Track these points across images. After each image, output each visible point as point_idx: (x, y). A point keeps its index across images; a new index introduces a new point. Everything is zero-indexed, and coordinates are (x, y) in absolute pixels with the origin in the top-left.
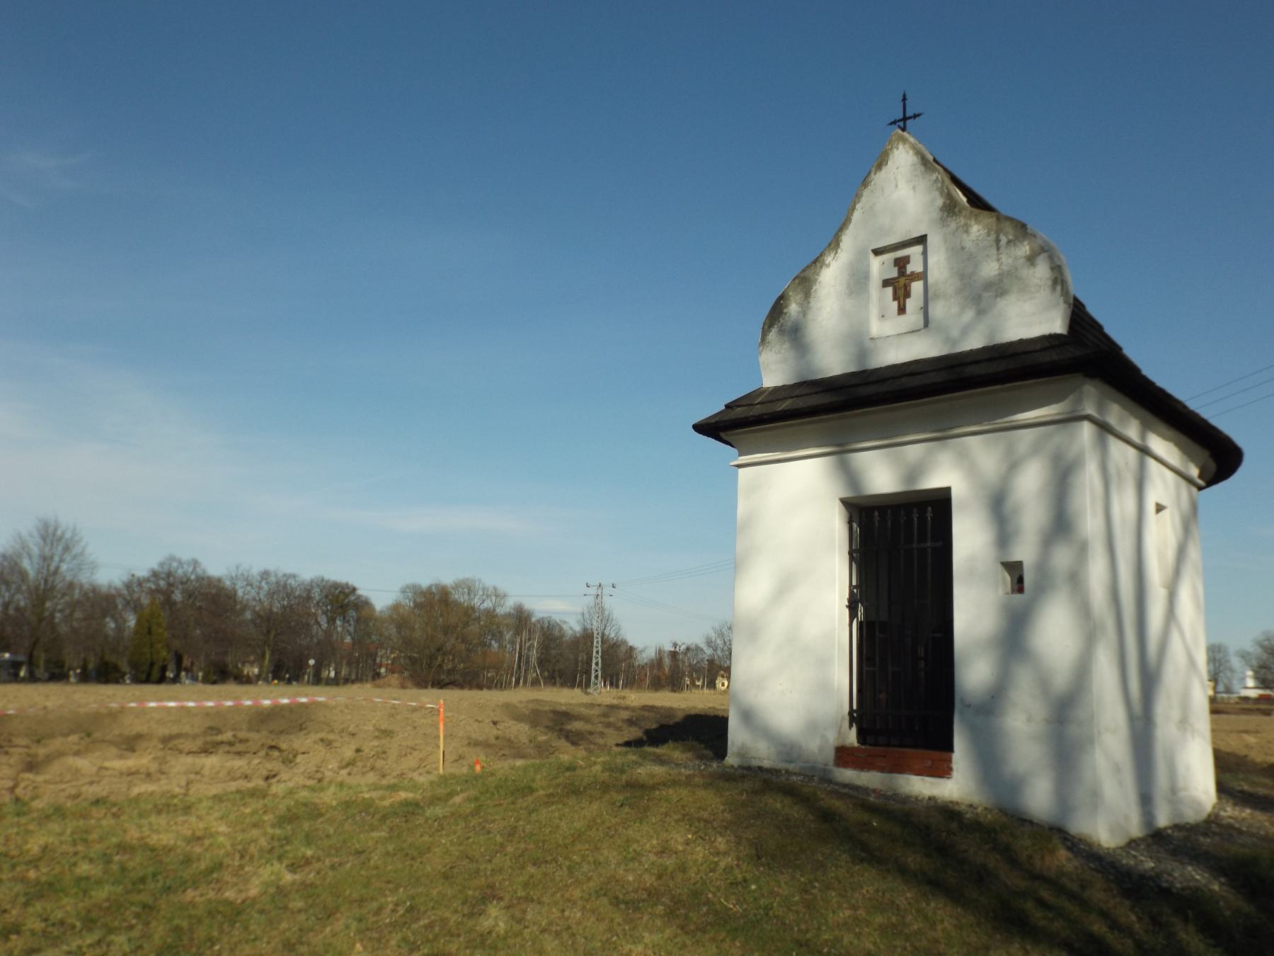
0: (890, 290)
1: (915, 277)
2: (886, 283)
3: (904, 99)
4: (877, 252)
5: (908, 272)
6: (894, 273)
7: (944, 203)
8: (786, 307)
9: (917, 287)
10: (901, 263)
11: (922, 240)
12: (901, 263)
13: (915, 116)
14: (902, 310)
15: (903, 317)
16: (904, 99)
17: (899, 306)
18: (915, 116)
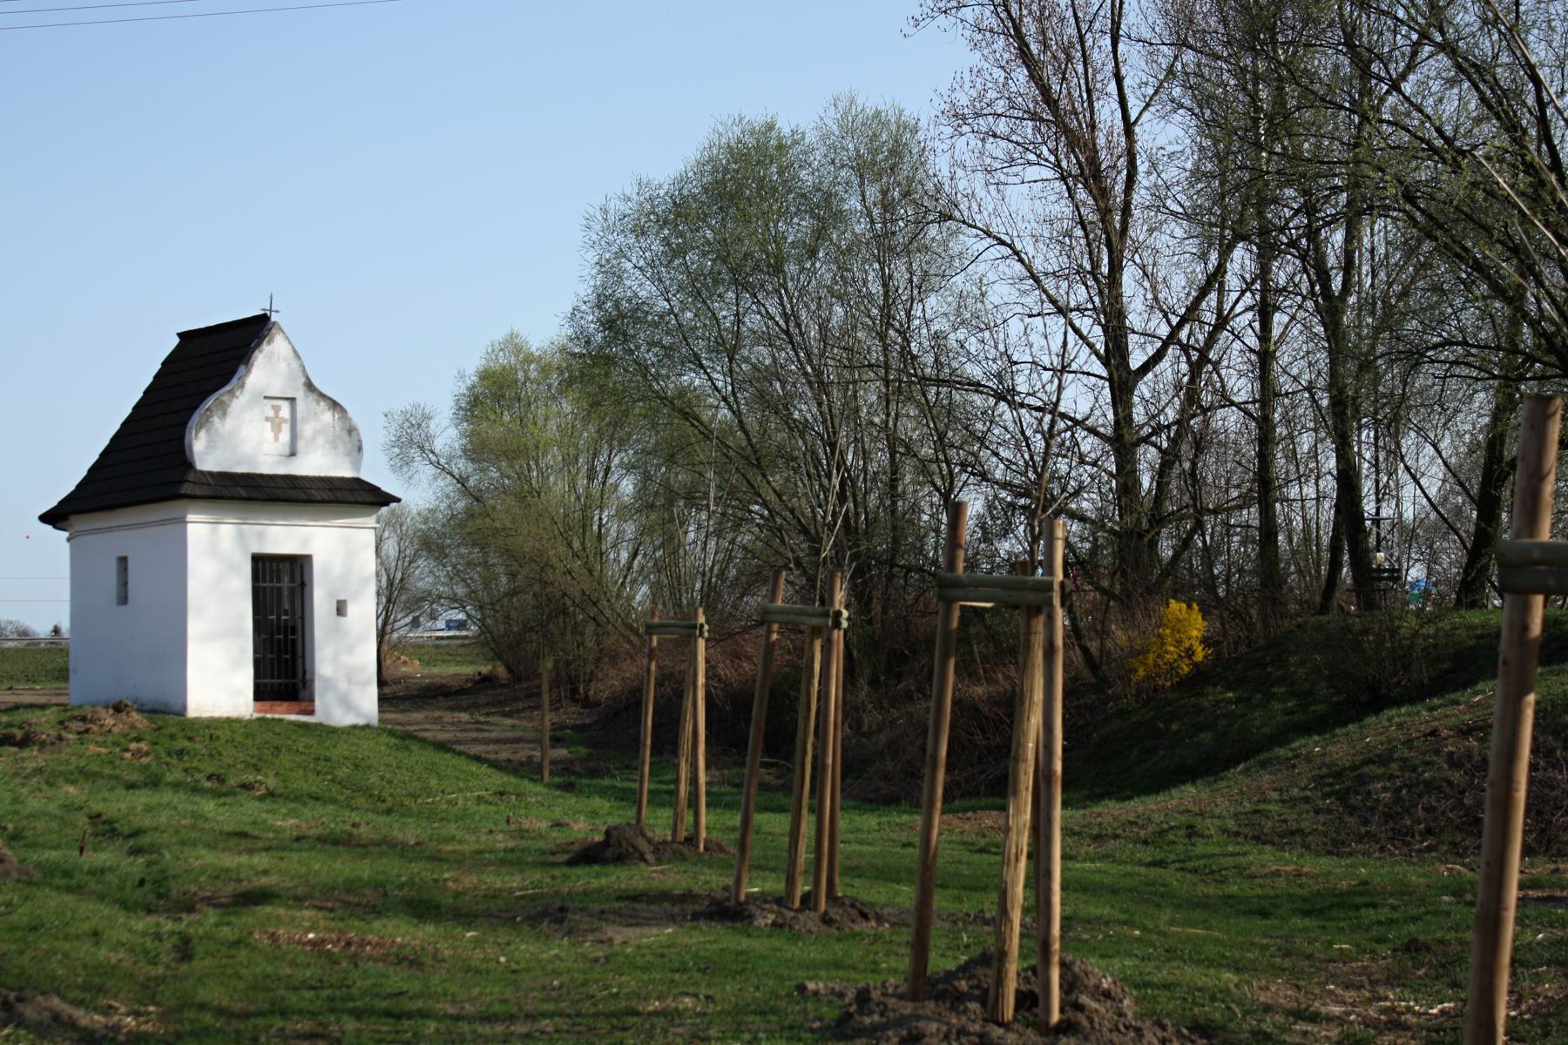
6: (271, 413)
10: (277, 409)
11: (292, 400)
14: (276, 439)
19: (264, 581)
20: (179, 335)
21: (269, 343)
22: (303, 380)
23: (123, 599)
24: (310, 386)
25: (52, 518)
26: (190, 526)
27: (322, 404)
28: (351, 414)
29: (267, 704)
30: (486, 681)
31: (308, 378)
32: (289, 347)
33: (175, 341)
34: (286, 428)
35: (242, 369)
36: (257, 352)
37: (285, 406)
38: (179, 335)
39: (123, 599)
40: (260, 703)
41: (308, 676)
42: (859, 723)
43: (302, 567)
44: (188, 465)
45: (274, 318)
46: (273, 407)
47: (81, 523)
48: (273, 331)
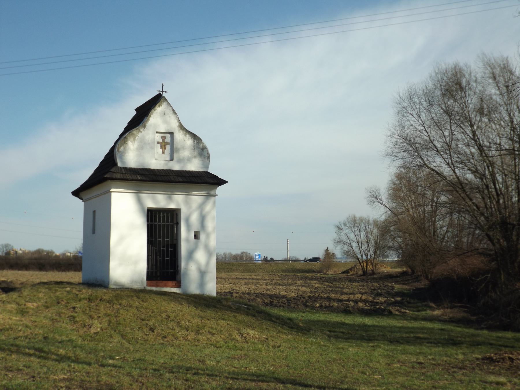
0: (159, 145)
1: (167, 143)
2: (158, 143)
3: (163, 85)
4: (157, 132)
5: (166, 141)
6: (161, 140)
7: (179, 126)
8: (127, 141)
9: (168, 147)
11: (172, 134)
12: (164, 138)
13: (166, 92)
14: (163, 153)
15: (163, 155)
16: (163, 85)
17: (163, 151)
18: (166, 92)
19: (167, 221)
20: (136, 110)
21: (159, 106)
22: (178, 124)
23: (94, 232)
24: (181, 127)
25: (76, 193)
26: (112, 193)
27: (188, 136)
28: (204, 140)
29: (154, 282)
30: (404, 273)
31: (180, 123)
32: (171, 108)
33: (135, 113)
34: (168, 147)
35: (146, 119)
36: (153, 110)
37: (168, 136)
38: (136, 110)
39: (94, 232)
40: (149, 282)
41: (179, 269)
42: (170, 328)
43: (177, 215)
44: (115, 164)
45: (164, 94)
46: (162, 137)
47: (86, 194)
48: (162, 100)
